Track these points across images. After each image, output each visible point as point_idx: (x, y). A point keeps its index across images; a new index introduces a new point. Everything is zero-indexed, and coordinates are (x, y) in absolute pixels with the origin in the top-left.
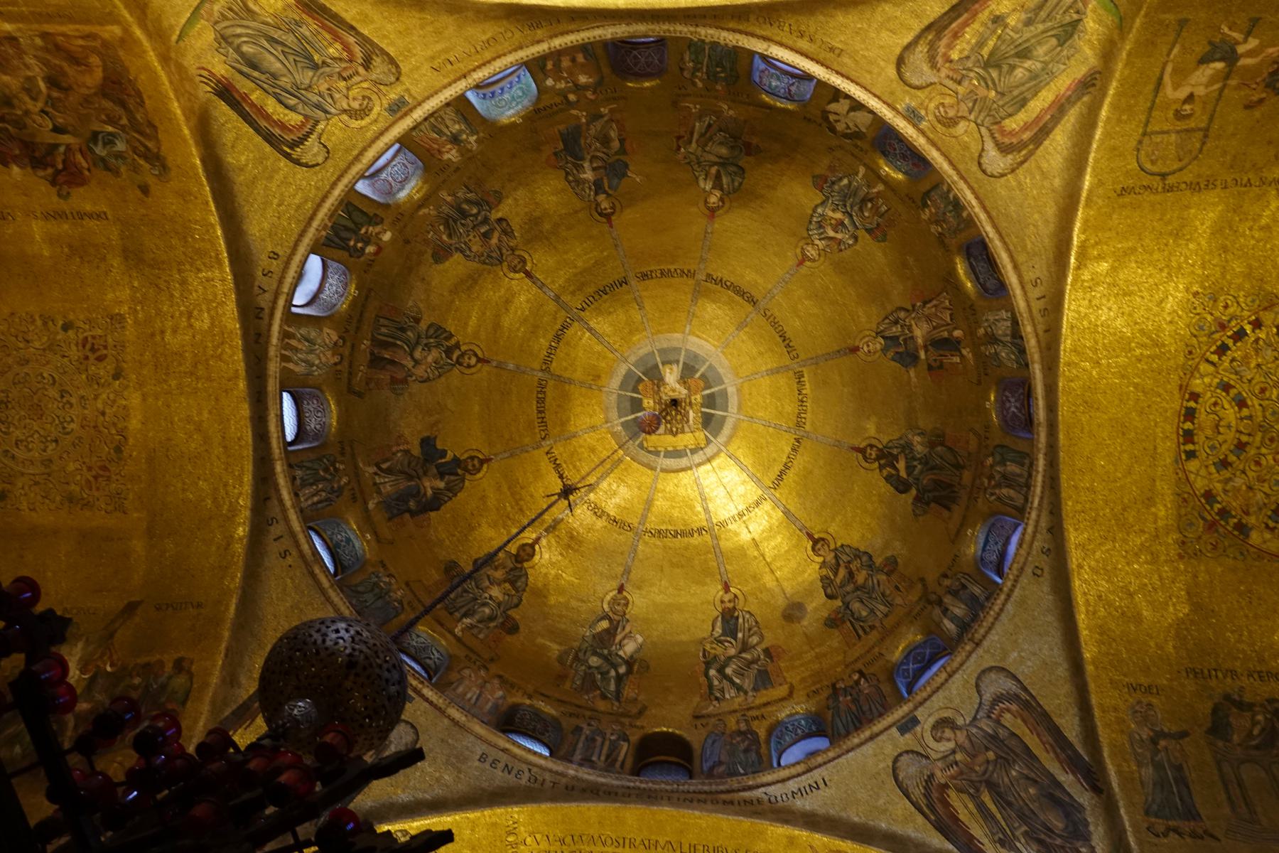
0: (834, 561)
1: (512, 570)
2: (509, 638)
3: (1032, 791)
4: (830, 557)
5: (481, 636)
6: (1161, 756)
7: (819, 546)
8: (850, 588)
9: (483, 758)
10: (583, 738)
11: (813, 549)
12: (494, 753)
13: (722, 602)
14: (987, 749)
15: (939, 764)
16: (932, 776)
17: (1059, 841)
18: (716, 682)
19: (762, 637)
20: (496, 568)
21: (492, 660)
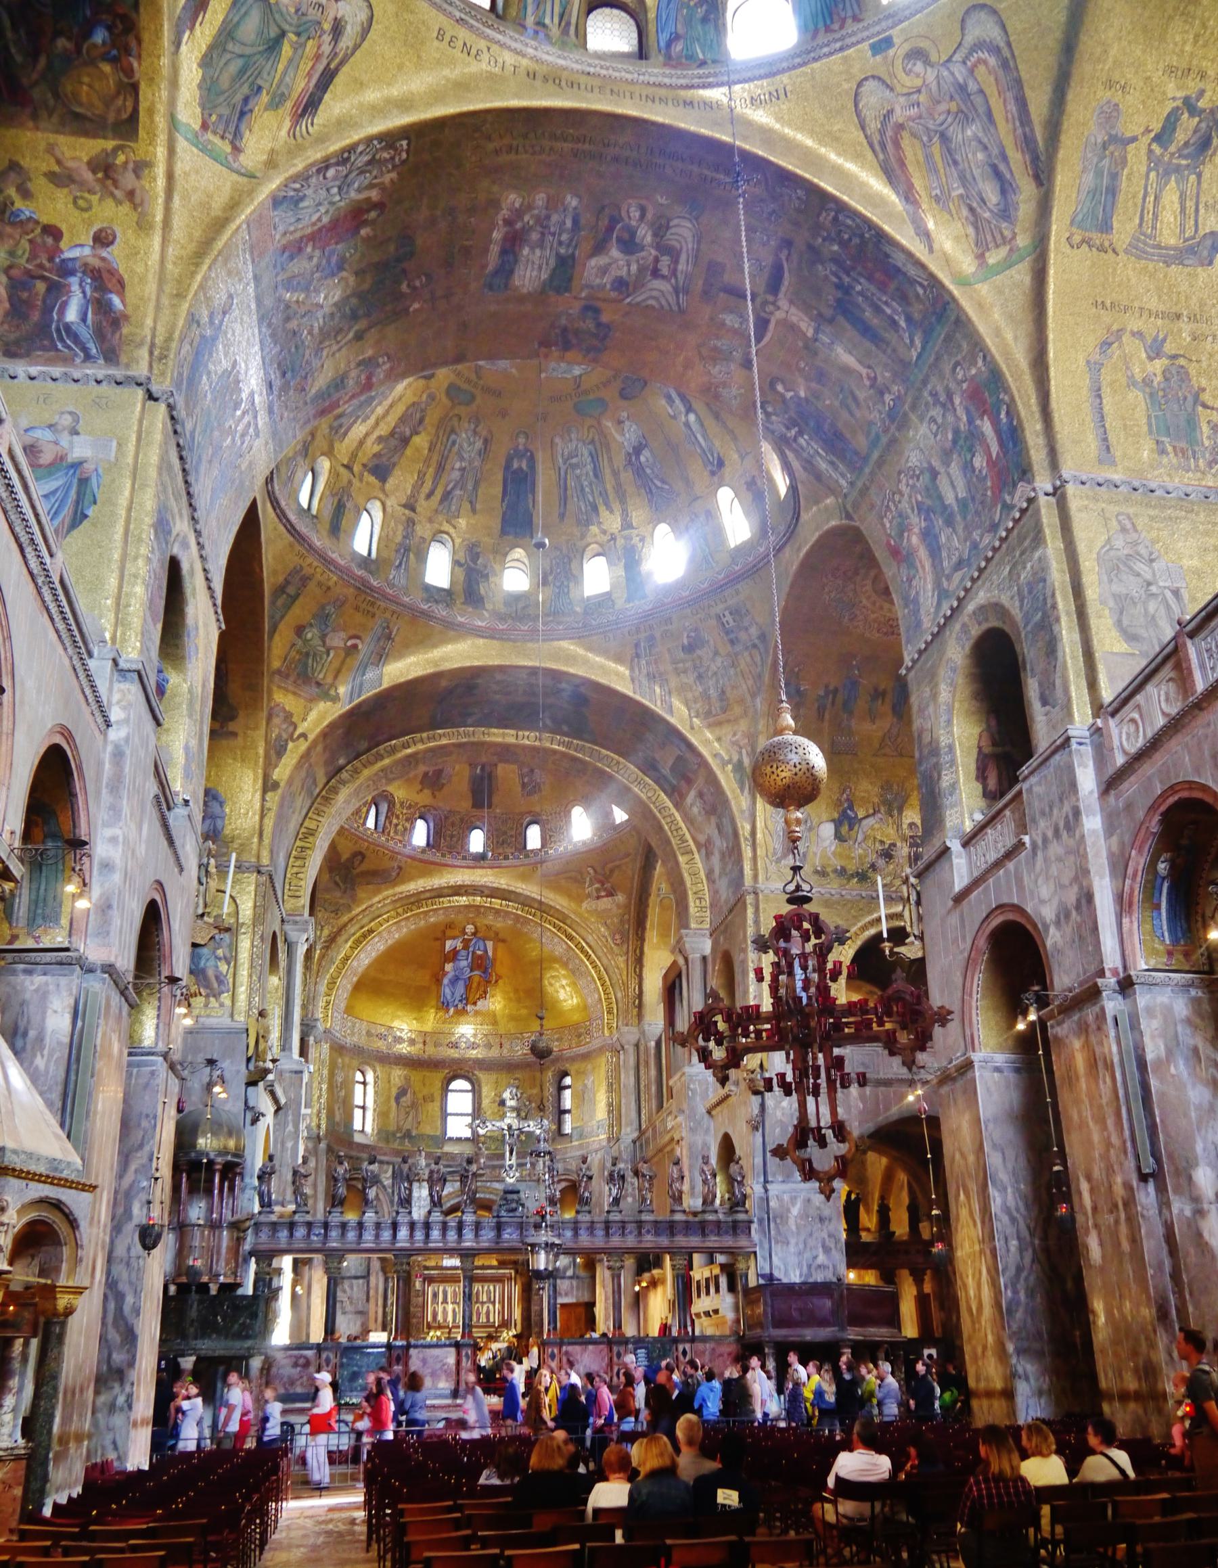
3: (980, 156)
6: (1106, 162)
9: (440, 35)
12: (451, 29)
15: (902, 100)
17: (987, 215)
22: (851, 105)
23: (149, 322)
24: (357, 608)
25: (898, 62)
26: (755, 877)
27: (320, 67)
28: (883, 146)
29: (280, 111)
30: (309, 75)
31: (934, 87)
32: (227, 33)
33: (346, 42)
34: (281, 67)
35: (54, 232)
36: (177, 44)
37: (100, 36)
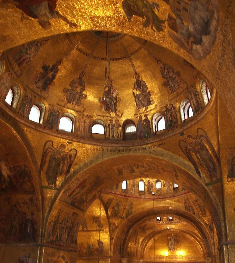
0: (163, 67)
1: (79, 82)
2: (86, 100)
4: (162, 66)
5: (79, 104)
7: (159, 62)
8: (168, 76)
10: (110, 128)
11: (158, 63)
13: (136, 78)
14: (199, 145)
15: (189, 145)
16: (187, 147)
17: (211, 170)
18: (138, 103)
19: (147, 88)
20: (76, 84)
21: (84, 111)
22: (178, 147)
23: (41, 230)
24: (124, 201)
25: (186, 137)
26: (215, 253)
27: (68, 165)
28: (187, 154)
29: (63, 175)
30: (67, 167)
31: (194, 142)
32: (49, 167)
33: (72, 159)
34: (61, 168)
35: (25, 213)
36: (40, 174)
37: (26, 178)
